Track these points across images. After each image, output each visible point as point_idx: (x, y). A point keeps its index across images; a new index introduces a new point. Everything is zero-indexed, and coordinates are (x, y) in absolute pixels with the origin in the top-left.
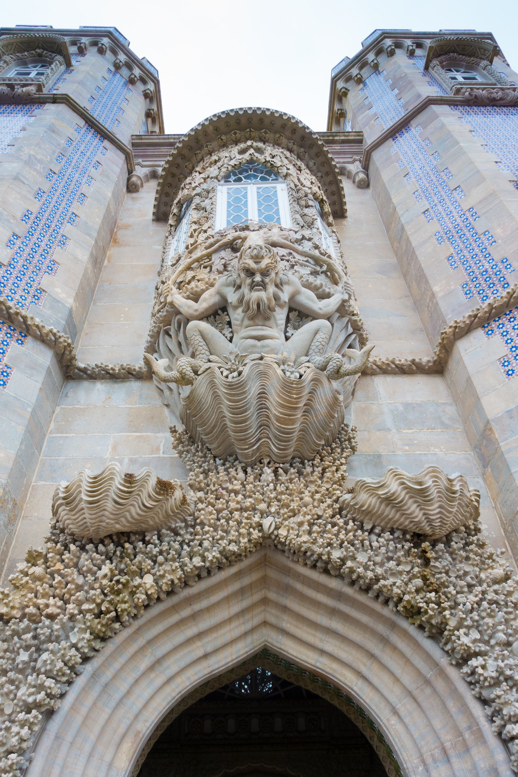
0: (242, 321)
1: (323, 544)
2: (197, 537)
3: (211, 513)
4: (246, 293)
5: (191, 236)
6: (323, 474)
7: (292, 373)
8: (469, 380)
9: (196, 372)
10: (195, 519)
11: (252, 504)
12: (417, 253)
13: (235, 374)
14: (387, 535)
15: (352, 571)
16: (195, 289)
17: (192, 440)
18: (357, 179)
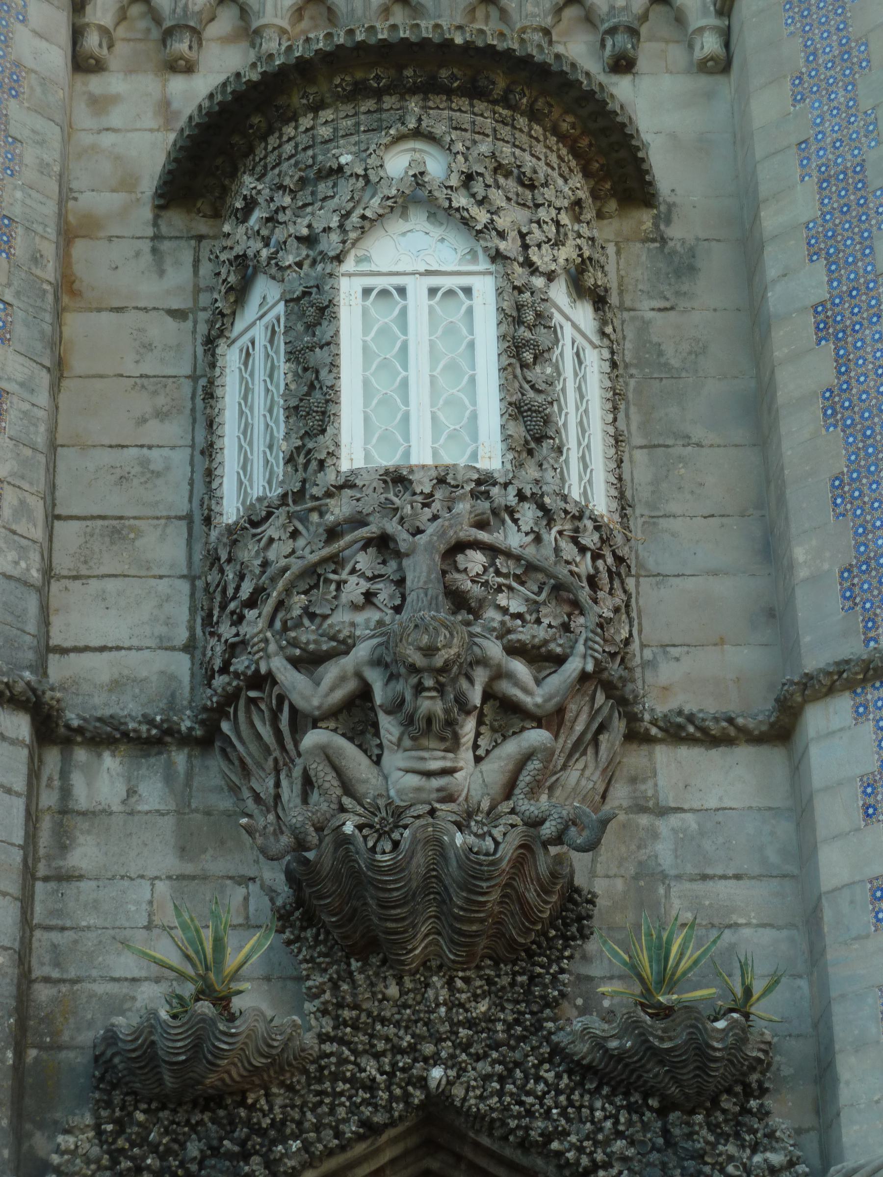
0: (400, 740)
1: (519, 1113)
2: (327, 1100)
3: (347, 1061)
4: (408, 697)
5: (290, 460)
6: (529, 985)
7: (482, 837)
8: (811, 796)
9: (319, 829)
10: (321, 1069)
11: (409, 1044)
12: (783, 430)
13: (388, 847)
14: (618, 1100)
15: (559, 1154)
16: (312, 647)
17: (310, 919)
18: (698, 55)
